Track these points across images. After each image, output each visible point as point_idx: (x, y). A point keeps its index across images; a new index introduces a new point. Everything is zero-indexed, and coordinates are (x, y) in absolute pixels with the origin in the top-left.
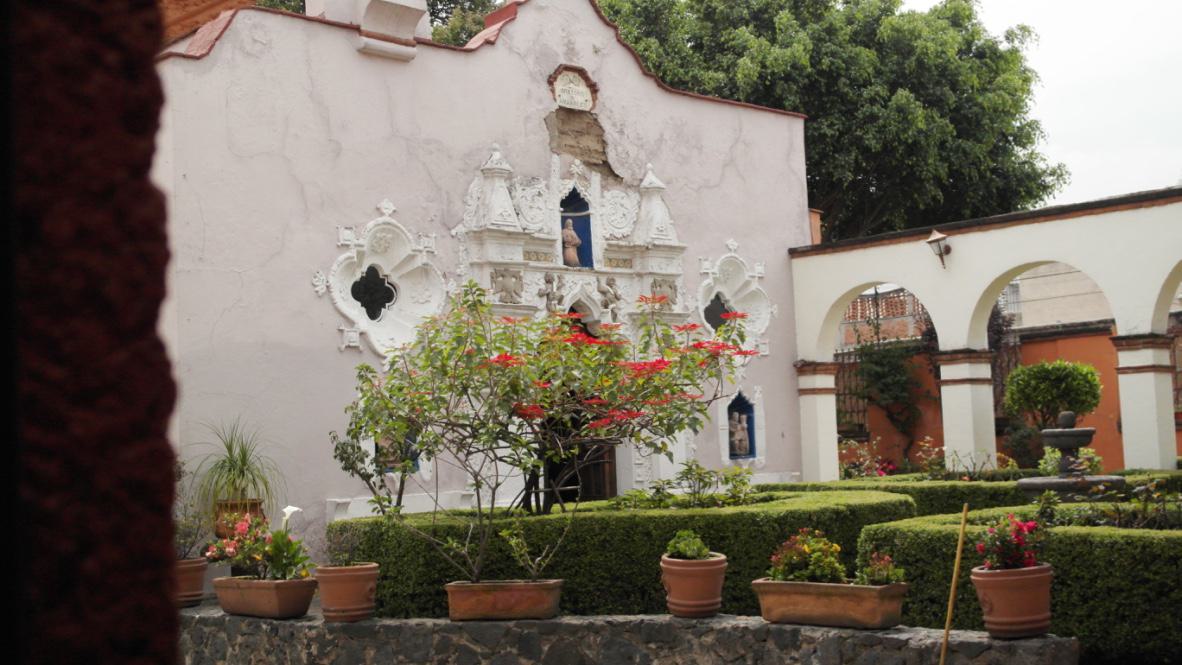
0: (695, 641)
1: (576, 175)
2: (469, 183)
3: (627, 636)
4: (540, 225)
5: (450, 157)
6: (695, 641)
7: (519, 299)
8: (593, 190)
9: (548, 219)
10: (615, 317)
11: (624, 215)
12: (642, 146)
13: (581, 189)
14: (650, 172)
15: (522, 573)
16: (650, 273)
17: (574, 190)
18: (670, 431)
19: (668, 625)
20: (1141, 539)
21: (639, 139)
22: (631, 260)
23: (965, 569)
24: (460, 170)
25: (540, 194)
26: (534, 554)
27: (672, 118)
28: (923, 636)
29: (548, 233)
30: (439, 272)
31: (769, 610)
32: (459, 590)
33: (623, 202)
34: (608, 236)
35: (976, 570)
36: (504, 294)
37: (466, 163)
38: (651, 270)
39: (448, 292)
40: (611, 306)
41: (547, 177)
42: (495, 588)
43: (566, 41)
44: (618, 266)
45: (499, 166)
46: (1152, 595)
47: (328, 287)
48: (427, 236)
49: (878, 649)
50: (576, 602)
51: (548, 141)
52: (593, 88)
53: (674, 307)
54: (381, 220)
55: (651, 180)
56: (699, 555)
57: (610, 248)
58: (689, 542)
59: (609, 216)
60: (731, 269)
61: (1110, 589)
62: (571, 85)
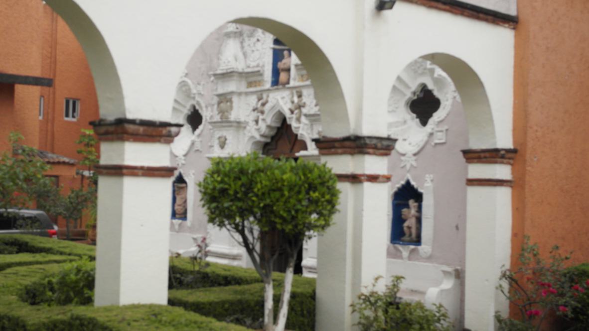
25: (258, 40)
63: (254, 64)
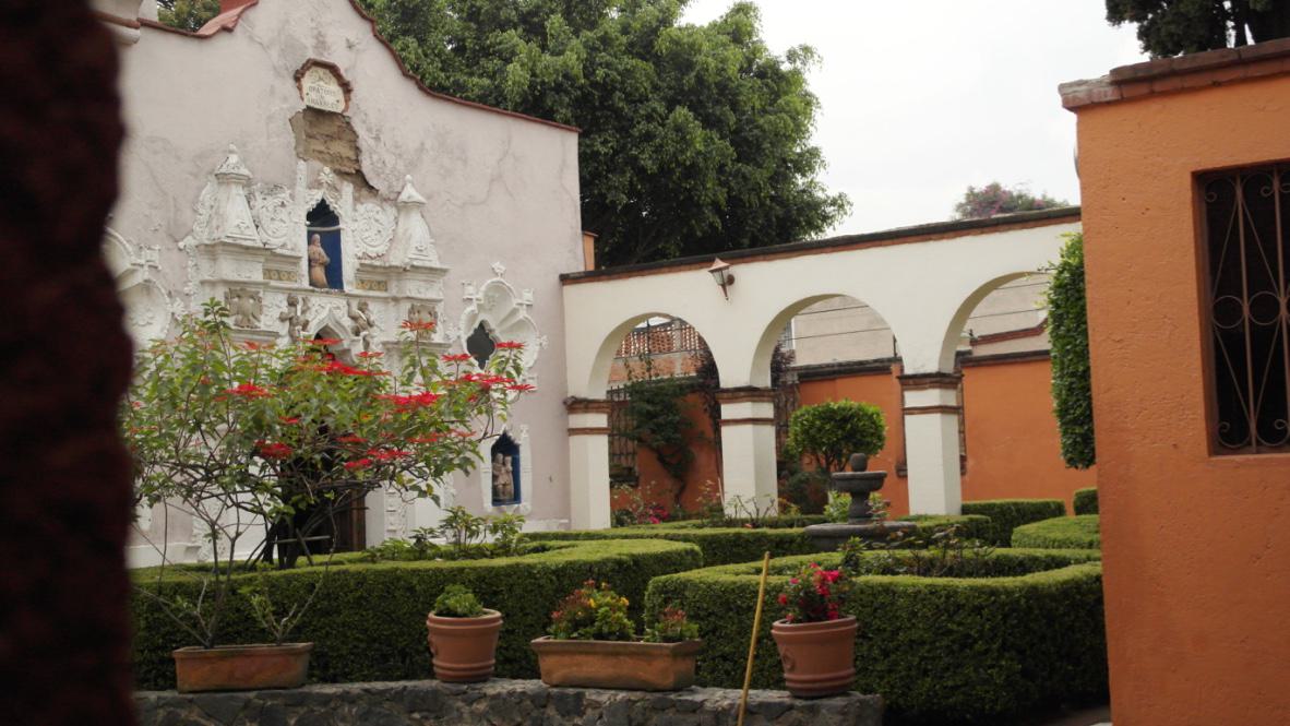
0: (466, 709)
2: (201, 189)
3: (387, 705)
4: (282, 240)
5: (178, 158)
6: (466, 709)
7: (257, 323)
8: (344, 202)
9: (292, 234)
11: (379, 232)
12: (400, 155)
14: (409, 185)
15: (264, 635)
16: (408, 298)
17: (323, 201)
18: (438, 473)
19: (435, 692)
20: (945, 587)
21: (397, 147)
22: (386, 283)
23: (765, 625)
24: (191, 174)
25: (283, 205)
26: (281, 612)
27: (434, 125)
28: (718, 697)
29: (292, 249)
30: (163, 291)
31: (549, 673)
32: (188, 658)
33: (378, 217)
34: (360, 254)
35: (776, 624)
36: (240, 317)
37: (198, 166)
38: (409, 294)
39: (173, 314)
40: (363, 333)
41: (292, 186)
42: (233, 655)
43: (315, 32)
44: (371, 289)
45: (236, 171)
46: (955, 647)
48: (149, 249)
49: (670, 714)
50: (326, 667)
51: (294, 145)
52: (346, 88)
53: (433, 336)
55: (410, 193)
56: (471, 612)
57: (363, 269)
58: (460, 598)
61: (912, 641)
62: (322, 83)
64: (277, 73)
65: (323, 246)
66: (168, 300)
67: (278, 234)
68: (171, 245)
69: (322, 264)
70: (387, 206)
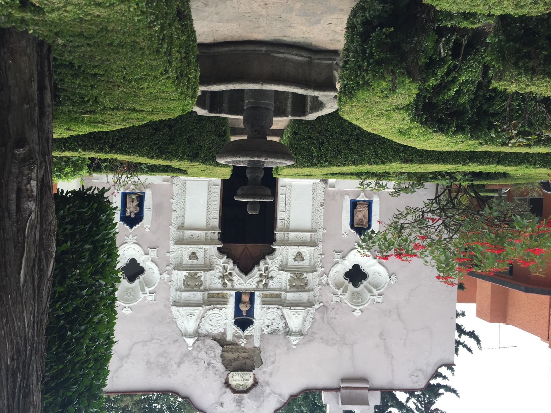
1: (243, 338)
4: (269, 311)
5: (322, 339)
7: (292, 275)
8: (232, 332)
9: (263, 316)
10: (225, 268)
12: (195, 358)
13: (240, 332)
14: (191, 345)
17: (243, 330)
21: (196, 362)
22: (208, 297)
24: (316, 333)
25: (268, 326)
27: (170, 377)
30: (332, 286)
33: (212, 327)
36: (301, 277)
40: (227, 273)
41: (262, 336)
43: (242, 406)
45: (298, 338)
47: (390, 277)
52: (227, 384)
53: (187, 274)
54: (361, 307)
55: (190, 341)
57: (225, 303)
59: (223, 319)
60: (126, 297)
62: (241, 384)
63: (271, 310)
64: (268, 384)
65: (242, 311)
66: (330, 283)
67: (271, 313)
68: (326, 304)
69: (244, 303)
70: (204, 332)
